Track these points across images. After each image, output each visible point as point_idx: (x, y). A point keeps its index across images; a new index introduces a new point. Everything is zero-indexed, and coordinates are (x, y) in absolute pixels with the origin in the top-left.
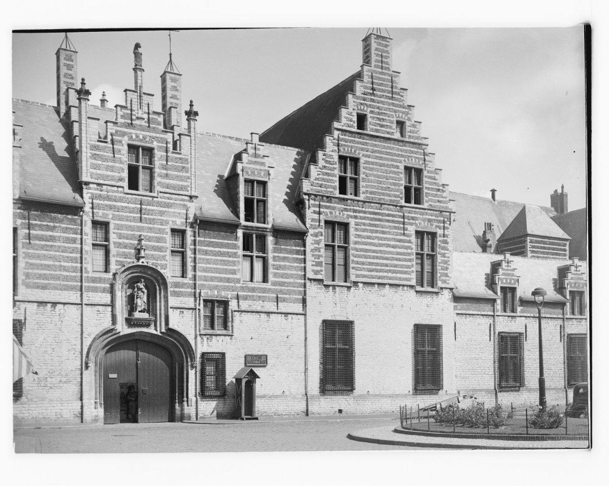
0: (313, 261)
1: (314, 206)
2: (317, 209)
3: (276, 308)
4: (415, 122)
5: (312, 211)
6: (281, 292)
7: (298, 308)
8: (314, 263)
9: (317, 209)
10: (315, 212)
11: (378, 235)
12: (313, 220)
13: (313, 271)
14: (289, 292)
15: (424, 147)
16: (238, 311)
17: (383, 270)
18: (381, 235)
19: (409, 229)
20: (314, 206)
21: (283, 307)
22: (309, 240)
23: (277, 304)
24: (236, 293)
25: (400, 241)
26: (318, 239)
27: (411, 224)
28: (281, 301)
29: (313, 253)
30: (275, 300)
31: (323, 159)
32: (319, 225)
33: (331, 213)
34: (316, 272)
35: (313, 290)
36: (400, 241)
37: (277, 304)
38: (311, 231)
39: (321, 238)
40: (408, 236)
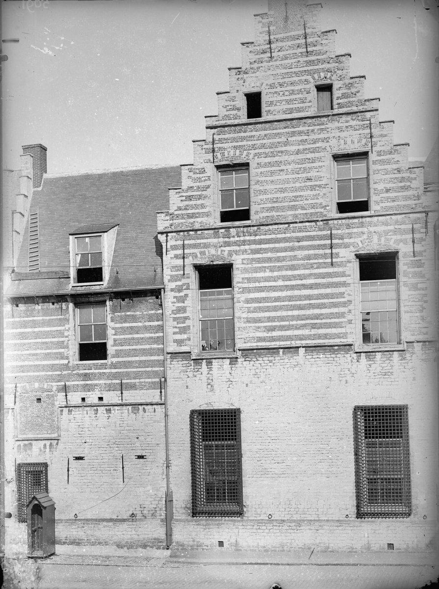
0: (176, 327)
1: (174, 248)
2: (180, 252)
3: (120, 398)
4: (352, 78)
5: (173, 256)
6: (128, 375)
7: (153, 395)
8: (177, 330)
9: (180, 252)
10: (176, 257)
11: (284, 273)
12: (174, 268)
13: (175, 341)
14: (137, 375)
15: (368, 115)
16: (66, 407)
17: (293, 325)
18: (290, 273)
19: (341, 255)
20: (174, 248)
21: (130, 396)
22: (169, 299)
23: (122, 393)
24: (64, 384)
25: (323, 276)
26: (182, 294)
27: (346, 246)
28: (126, 389)
29: (175, 316)
30: (119, 387)
31: (189, 177)
32: (184, 274)
33: (203, 253)
34: (179, 342)
35: (175, 369)
36: (323, 276)
37: (122, 393)
38: (170, 285)
39: (185, 292)
40: (340, 265)
